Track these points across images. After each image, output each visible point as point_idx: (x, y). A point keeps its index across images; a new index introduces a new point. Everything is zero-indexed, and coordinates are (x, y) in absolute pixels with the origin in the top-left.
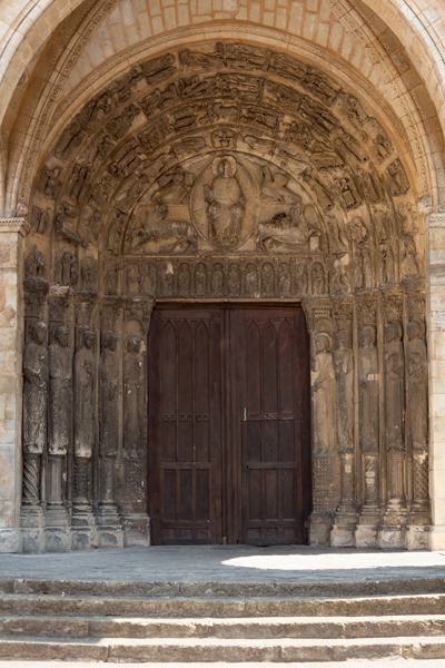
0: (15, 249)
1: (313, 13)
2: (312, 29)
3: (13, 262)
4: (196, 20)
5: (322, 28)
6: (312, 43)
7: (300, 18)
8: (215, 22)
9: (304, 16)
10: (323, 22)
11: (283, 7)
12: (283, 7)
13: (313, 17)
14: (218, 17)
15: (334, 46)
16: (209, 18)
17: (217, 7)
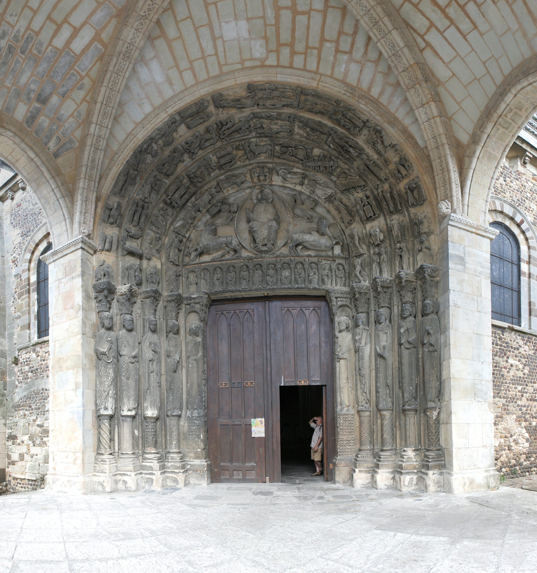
0: (80, 261)
1: (345, 52)
2: (342, 70)
3: (79, 270)
4: (225, 69)
5: (354, 68)
6: (343, 82)
7: (332, 58)
8: (244, 69)
9: (335, 56)
10: (356, 62)
11: (314, 48)
12: (314, 48)
13: (345, 57)
14: (248, 64)
15: (365, 85)
16: (239, 66)
17: (246, 56)
